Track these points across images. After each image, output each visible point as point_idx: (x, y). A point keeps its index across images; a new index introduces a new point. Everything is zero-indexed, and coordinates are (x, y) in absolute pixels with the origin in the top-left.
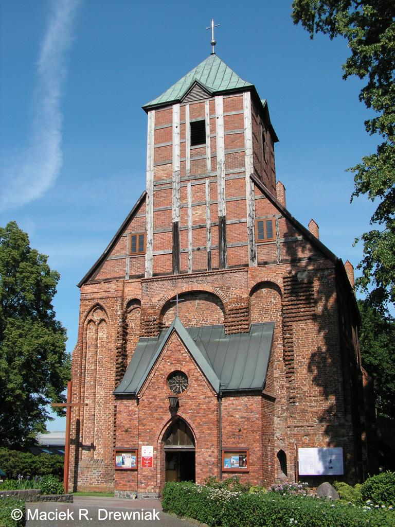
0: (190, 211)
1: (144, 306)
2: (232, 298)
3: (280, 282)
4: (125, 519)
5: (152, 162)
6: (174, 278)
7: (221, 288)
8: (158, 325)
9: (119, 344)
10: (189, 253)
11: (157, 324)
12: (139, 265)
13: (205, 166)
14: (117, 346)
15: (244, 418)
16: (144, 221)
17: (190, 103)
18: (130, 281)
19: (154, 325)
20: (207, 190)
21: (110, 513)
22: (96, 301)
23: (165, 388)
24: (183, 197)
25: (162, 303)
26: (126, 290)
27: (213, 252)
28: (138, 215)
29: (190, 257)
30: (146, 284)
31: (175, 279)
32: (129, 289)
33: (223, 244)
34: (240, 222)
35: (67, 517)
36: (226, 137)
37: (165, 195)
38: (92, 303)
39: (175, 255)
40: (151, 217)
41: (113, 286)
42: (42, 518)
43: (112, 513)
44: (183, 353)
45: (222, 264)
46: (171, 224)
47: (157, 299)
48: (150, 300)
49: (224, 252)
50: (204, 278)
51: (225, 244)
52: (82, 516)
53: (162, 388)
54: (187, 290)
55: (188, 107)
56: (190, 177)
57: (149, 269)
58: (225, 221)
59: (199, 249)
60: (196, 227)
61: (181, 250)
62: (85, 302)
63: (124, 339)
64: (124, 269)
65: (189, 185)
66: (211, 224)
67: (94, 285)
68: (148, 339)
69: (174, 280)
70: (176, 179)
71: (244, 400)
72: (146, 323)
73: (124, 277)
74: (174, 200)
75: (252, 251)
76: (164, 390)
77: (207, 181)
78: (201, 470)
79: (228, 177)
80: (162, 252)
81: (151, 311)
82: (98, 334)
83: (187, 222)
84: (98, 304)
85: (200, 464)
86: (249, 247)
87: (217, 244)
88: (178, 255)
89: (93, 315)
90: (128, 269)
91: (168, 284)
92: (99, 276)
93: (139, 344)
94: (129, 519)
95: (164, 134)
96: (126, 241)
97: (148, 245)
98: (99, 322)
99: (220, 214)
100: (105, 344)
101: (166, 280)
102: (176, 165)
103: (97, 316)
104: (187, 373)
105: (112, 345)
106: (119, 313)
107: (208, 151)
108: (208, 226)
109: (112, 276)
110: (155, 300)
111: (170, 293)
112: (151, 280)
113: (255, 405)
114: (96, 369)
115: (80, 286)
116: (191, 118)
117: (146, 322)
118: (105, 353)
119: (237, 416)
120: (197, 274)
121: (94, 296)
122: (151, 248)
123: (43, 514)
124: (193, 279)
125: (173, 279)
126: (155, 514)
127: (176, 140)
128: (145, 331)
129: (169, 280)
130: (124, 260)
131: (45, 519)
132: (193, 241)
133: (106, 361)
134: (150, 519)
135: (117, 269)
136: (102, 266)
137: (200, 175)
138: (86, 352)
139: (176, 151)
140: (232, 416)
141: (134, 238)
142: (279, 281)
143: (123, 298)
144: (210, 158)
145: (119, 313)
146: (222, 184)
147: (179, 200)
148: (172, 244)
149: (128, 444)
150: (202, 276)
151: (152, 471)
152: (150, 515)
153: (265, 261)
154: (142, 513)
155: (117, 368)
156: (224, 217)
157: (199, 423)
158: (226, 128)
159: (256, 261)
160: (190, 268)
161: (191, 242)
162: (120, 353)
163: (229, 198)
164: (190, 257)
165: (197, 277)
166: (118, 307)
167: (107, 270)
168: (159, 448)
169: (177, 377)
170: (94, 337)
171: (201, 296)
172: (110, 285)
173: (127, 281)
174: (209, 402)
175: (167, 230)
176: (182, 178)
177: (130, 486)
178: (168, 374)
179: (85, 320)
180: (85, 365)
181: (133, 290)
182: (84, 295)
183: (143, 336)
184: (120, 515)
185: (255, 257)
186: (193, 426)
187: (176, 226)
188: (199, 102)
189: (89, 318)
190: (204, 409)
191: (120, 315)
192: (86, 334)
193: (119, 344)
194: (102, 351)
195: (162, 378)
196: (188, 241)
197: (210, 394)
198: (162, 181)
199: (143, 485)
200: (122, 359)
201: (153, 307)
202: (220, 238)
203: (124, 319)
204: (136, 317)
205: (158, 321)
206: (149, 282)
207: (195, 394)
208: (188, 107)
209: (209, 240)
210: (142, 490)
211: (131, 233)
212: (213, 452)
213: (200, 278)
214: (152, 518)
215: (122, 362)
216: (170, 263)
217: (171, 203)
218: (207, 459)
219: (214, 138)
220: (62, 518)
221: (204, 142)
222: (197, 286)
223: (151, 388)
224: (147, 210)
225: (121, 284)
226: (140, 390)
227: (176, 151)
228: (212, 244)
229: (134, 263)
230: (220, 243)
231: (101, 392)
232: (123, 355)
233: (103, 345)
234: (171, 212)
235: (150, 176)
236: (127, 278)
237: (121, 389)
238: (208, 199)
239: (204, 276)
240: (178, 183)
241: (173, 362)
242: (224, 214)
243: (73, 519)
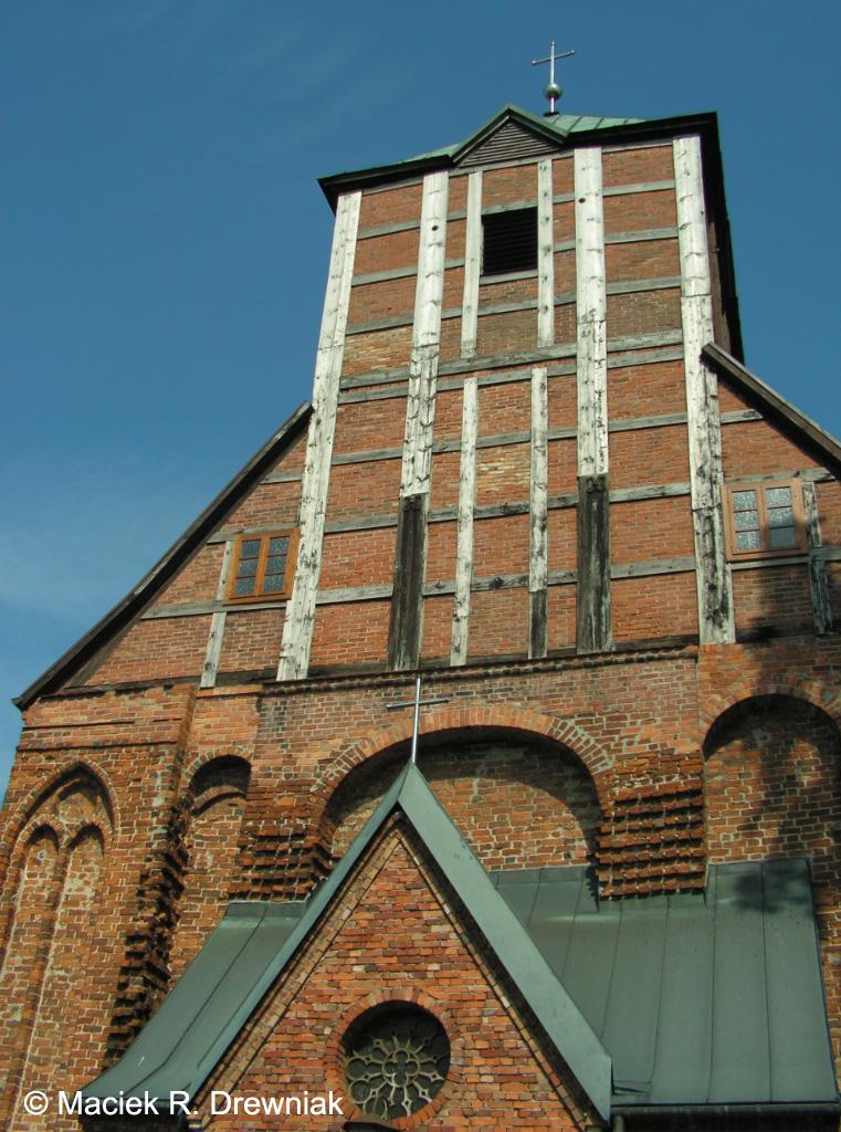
0: (468, 464)
1: (263, 782)
2: (630, 757)
4: (268, 1112)
5: (342, 324)
6: (390, 678)
7: (586, 718)
8: (313, 854)
9: (142, 923)
10: (460, 596)
11: (307, 850)
12: (258, 637)
13: (533, 329)
16: (296, 495)
17: (486, 168)
18: (216, 692)
19: (296, 851)
20: (538, 400)
21: (237, 1100)
22: (76, 756)
24: (447, 421)
25: (336, 772)
26: (198, 724)
28: (274, 476)
29: (463, 612)
30: (279, 700)
31: (397, 685)
32: (208, 721)
33: (594, 565)
35: (143, 1108)
36: (611, 250)
37: (379, 416)
38: (60, 764)
39: (403, 602)
40: (319, 482)
41: (149, 706)
42: (91, 1110)
43: (242, 1099)
46: (396, 504)
49: (601, 591)
50: (516, 682)
51: (602, 567)
52: (175, 1106)
55: (476, 181)
56: (476, 363)
57: (296, 649)
58: (604, 490)
59: (497, 585)
60: (491, 511)
61: (427, 587)
62: (34, 757)
64: (201, 650)
65: (470, 387)
66: (550, 500)
67: (78, 702)
68: (266, 908)
69: (391, 690)
70: (422, 368)
72: (262, 845)
73: (198, 678)
74: (412, 428)
75: (712, 588)
77: (539, 374)
79: (618, 361)
80: (350, 594)
81: (288, 800)
82: (62, 880)
83: (455, 496)
84: (81, 769)
86: (701, 575)
87: (568, 567)
88: (414, 603)
89: (55, 811)
90: (213, 650)
91: (366, 703)
92: (105, 673)
93: (224, 924)
94: (278, 1112)
95: (389, 250)
96: (223, 558)
97: (302, 570)
98: (74, 835)
99: (585, 470)
100: (83, 922)
101: (360, 687)
102: (427, 321)
103: (67, 816)
105: (113, 928)
106: (158, 802)
107: (546, 295)
109: (154, 672)
110: (308, 760)
111: (372, 734)
112: (297, 688)
115: (23, 705)
116: (485, 203)
117: (262, 838)
118: (80, 958)
120: (482, 668)
121: (73, 737)
122: (312, 580)
123: (94, 1102)
124: (468, 687)
125: (388, 684)
126: (334, 1101)
128: (256, 875)
129: (370, 686)
130: (204, 619)
131: (98, 1112)
132: (475, 556)
133: (77, 992)
134: (323, 1112)
135: (174, 648)
136: (121, 639)
137: (512, 354)
141: (249, 547)
143: (180, 749)
144: (551, 307)
145: (158, 802)
146: (593, 379)
147: (430, 430)
148: (394, 568)
150: (507, 674)
152: (323, 1105)
154: (306, 1099)
156: (602, 478)
158: (608, 228)
159: (729, 626)
160: (457, 650)
161: (470, 559)
162: (139, 955)
163: (622, 423)
164: (463, 612)
165: (487, 676)
166: (159, 782)
167: (132, 654)
170: (46, 894)
171: (499, 755)
172: (138, 702)
173: (207, 693)
175: (381, 520)
176: (446, 366)
178: (351, 1017)
179: (22, 826)
181: (223, 726)
182: (35, 733)
183: (243, 895)
184: (258, 1105)
185: (724, 608)
187: (413, 507)
188: (516, 163)
189: (37, 820)
191: (160, 808)
192: (17, 879)
193: (142, 923)
194: (68, 949)
195: (319, 1034)
196: (456, 557)
198: (369, 377)
200: (146, 982)
202: (584, 547)
203: (175, 830)
205: (312, 839)
206: (291, 693)
208: (476, 181)
209: (540, 553)
211: (240, 532)
213: (500, 681)
214: (328, 1110)
215: (142, 997)
217: (400, 439)
219: (566, 259)
220: (134, 1109)
221: (530, 262)
222: (483, 709)
223: (259, 1080)
224: (308, 462)
228: (551, 566)
229: (241, 629)
230: (583, 563)
232: (151, 968)
233: (77, 928)
234: (399, 468)
235: (328, 365)
236: (208, 680)
238: (539, 422)
239: (517, 674)
240: (430, 380)
242: (603, 467)
243: (156, 1113)
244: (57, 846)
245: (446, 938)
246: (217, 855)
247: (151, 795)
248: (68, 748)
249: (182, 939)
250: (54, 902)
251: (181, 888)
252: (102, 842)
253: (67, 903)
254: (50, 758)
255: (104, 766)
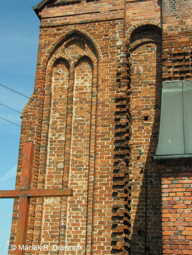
22: (72, 28)
38: (65, 31)
62: (50, 30)
98: (76, 61)
103: (72, 53)
121: (68, 20)
166: (118, 35)
170: (66, 86)
179: (49, 59)
191: (121, 46)
192: (51, 81)
247: (114, 41)
248: (67, 25)
250: (71, 89)
253: (77, 89)
255: (87, 31)
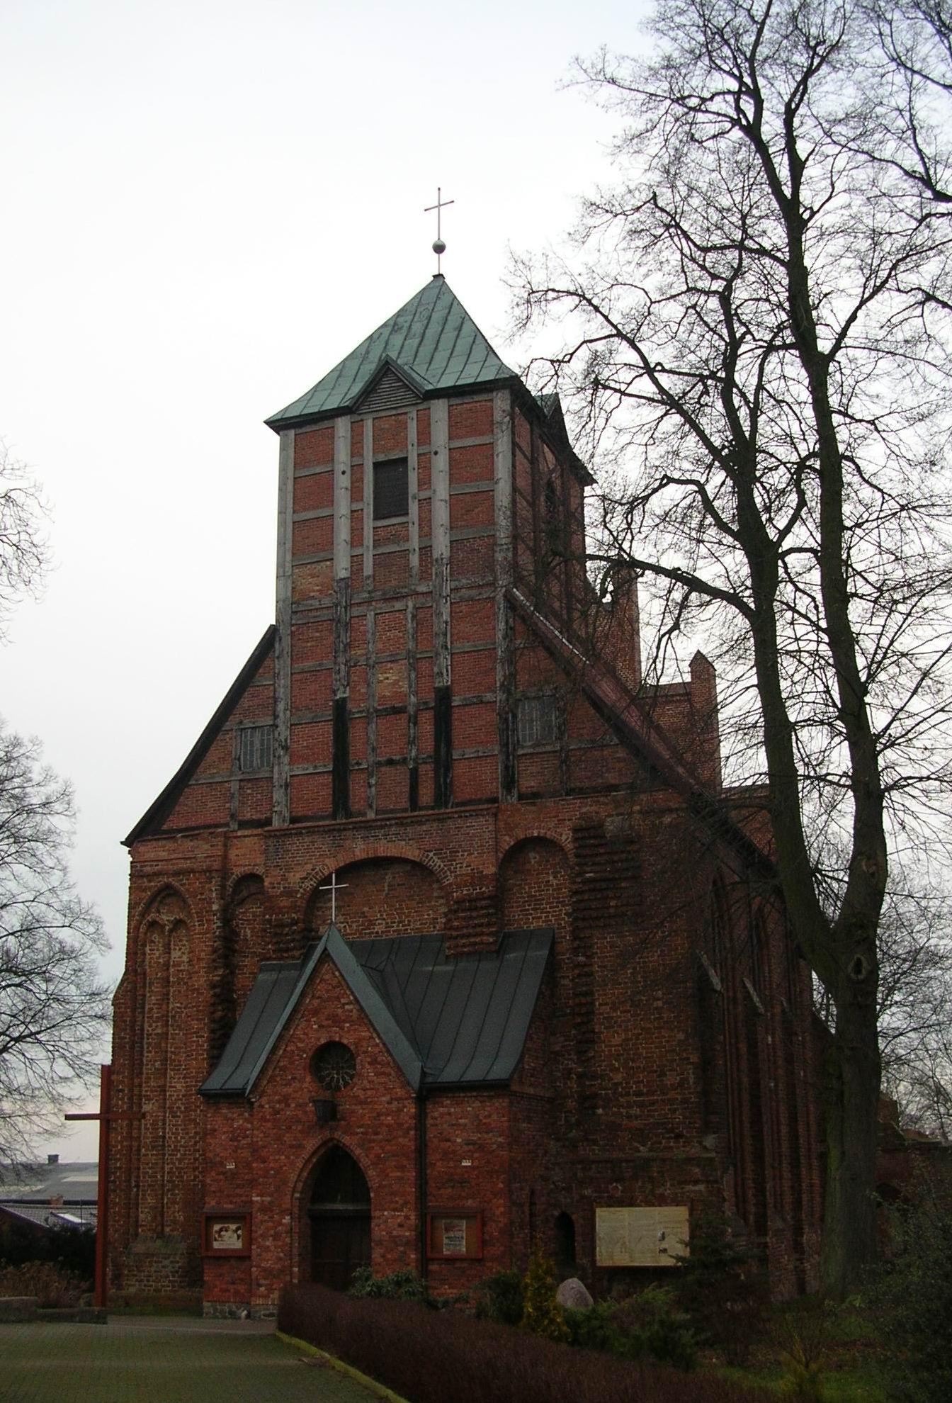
3: (566, 837)
14: (211, 982)
15: (474, 1144)
18: (239, 834)
23: (308, 1079)
26: (233, 854)
27: (423, 769)
32: (237, 852)
34: (482, 702)
44: (344, 1004)
45: (443, 796)
47: (298, 876)
48: (284, 878)
53: (302, 1080)
54: (364, 856)
63: (226, 966)
71: (472, 1106)
76: (305, 1085)
78: (383, 1256)
85: (380, 1243)
89: (158, 911)
104: (352, 1048)
105: (201, 980)
106: (215, 907)
108: (411, 710)
109: (201, 822)
112: (284, 834)
113: (495, 1117)
114: (167, 1034)
119: (459, 1140)
127: (343, 506)
138: (144, 996)
139: (343, 532)
140: (448, 1140)
142: (564, 837)
143: (224, 872)
145: (215, 907)
149: (231, 1203)
151: (280, 1259)
153: (534, 790)
155: (213, 1031)
157: (378, 1156)
168: (296, 1210)
169: (331, 1057)
172: (195, 843)
174: (400, 1110)
177: (237, 1292)
180: (142, 1026)
186: (364, 1162)
190: (388, 1126)
197: (400, 1092)
199: (262, 1289)
201: (289, 893)
203: (227, 918)
204: (254, 914)
207: (369, 1093)
210: (260, 1301)
212: (407, 1217)
216: (327, 793)
218: (395, 1233)
225: (219, 841)
226: (255, 1085)
227: (343, 532)
230: (437, 747)
231: (178, 1086)
237: (214, 1083)
241: (325, 1023)
244: (163, 932)
245: (351, 1011)
246: (252, 930)
249: (241, 980)
250: (167, 966)
251: (236, 951)
252: (188, 929)
254: (150, 881)
